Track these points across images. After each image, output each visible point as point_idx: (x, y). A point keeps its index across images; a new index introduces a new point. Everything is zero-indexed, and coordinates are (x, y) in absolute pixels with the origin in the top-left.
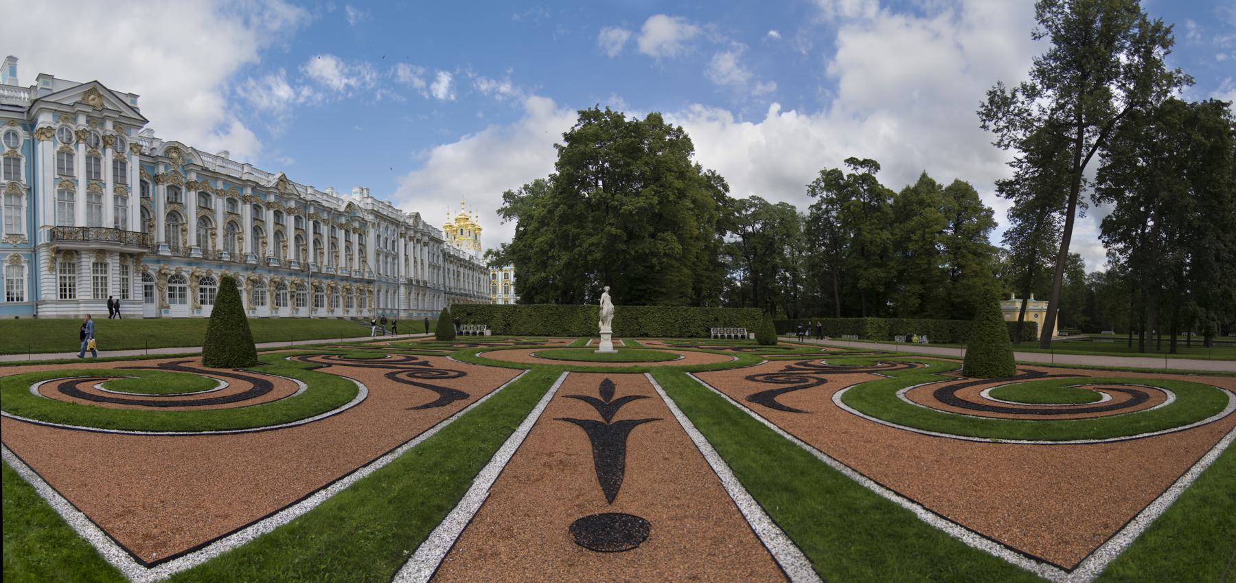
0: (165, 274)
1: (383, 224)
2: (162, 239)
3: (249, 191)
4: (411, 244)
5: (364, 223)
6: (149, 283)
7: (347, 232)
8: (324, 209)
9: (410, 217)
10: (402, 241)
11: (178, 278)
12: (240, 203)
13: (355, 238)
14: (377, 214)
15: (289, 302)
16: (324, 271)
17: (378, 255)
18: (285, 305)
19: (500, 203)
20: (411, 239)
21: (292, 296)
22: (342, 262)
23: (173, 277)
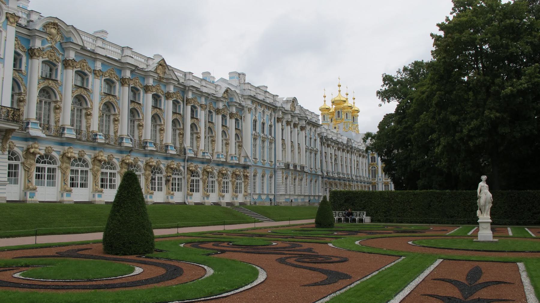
0: (34, 154)
1: (260, 109)
2: (33, 115)
3: (128, 74)
4: (288, 129)
5: (241, 108)
6: (14, 162)
7: (224, 117)
8: (202, 94)
9: (287, 101)
10: (279, 126)
11: (47, 158)
12: (118, 85)
13: (231, 123)
14: (253, 99)
15: (164, 187)
16: (200, 155)
17: (255, 139)
18: (160, 189)
20: (288, 123)
21: (167, 181)
22: (219, 146)
23: (41, 157)
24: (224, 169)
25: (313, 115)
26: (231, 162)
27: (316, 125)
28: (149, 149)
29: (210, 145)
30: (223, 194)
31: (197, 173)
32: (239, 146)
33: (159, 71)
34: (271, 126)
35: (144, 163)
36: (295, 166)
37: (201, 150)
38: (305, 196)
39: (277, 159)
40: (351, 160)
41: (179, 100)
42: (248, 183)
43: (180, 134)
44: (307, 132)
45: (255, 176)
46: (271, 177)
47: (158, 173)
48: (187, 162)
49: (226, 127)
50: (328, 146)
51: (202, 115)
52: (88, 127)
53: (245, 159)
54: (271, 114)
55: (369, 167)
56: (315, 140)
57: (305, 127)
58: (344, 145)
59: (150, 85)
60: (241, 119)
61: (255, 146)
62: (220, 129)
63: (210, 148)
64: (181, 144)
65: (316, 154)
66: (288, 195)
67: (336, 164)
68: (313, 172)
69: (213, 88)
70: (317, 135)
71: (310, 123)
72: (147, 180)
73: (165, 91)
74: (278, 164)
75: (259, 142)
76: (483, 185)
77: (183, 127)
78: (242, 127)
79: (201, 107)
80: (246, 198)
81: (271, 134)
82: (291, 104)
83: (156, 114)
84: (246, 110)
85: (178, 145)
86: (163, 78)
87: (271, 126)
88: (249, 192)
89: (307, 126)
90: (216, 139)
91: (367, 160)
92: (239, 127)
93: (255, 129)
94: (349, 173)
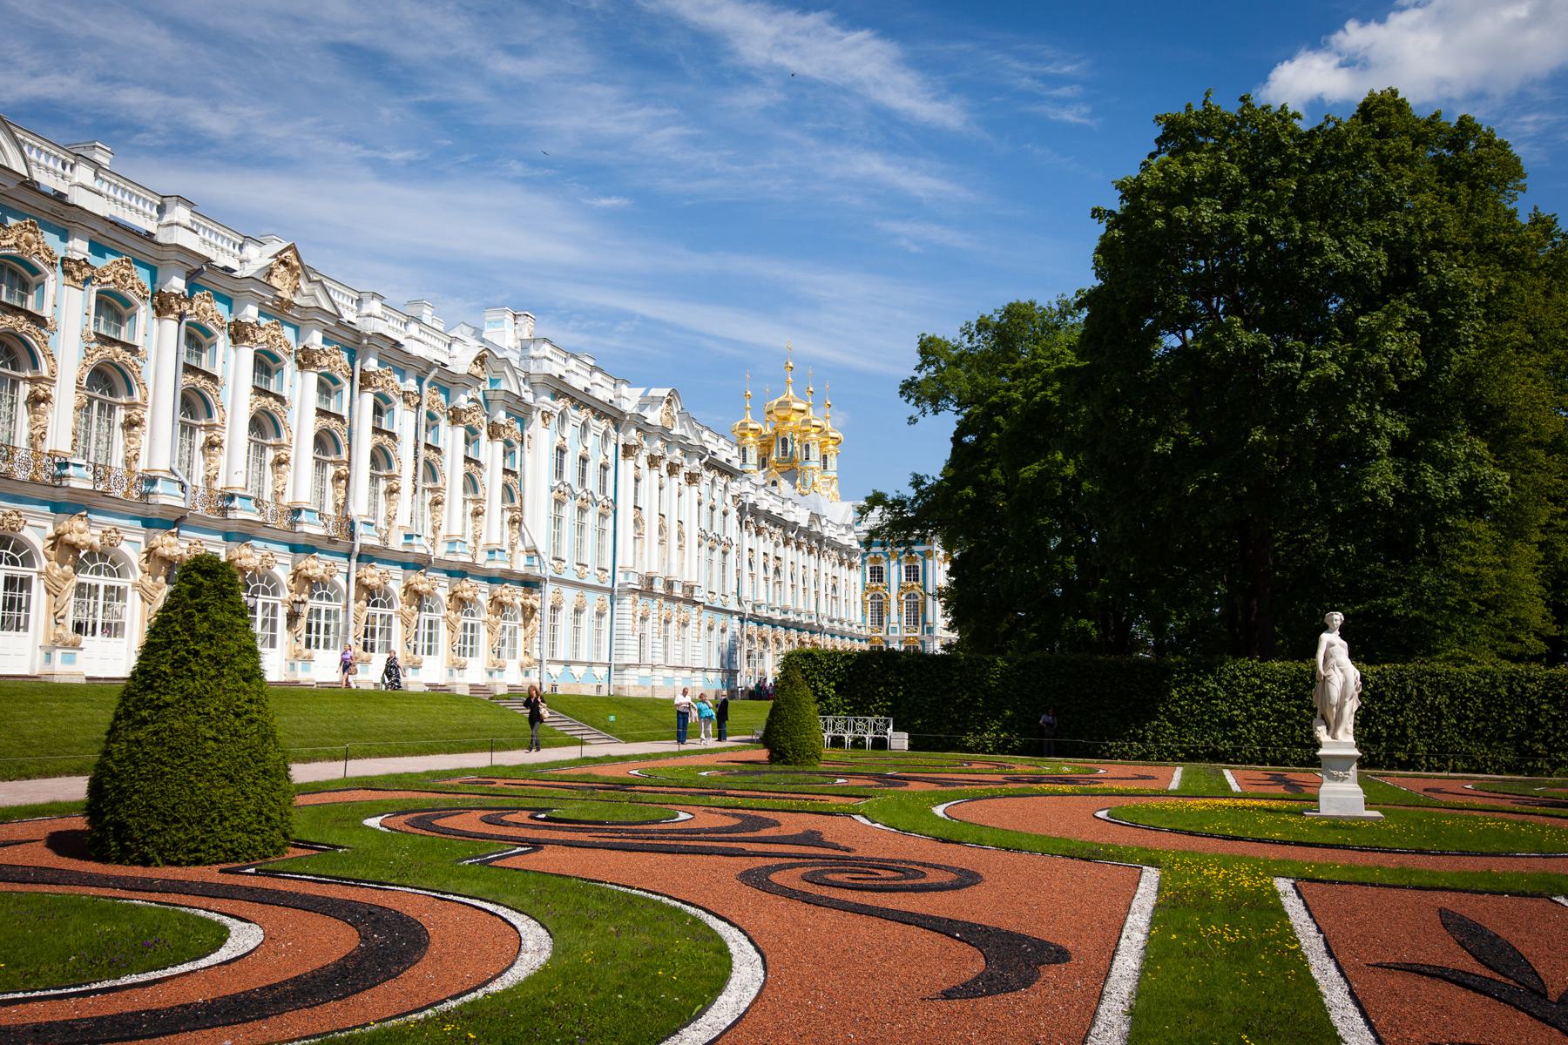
1: (577, 416)
4: (651, 478)
7: (471, 436)
10: (627, 468)
20: (653, 461)
21: (293, 617)
24: (467, 587)
26: (488, 566)
29: (428, 515)
31: (387, 595)
32: (513, 522)
36: (669, 585)
38: (694, 670)
39: (619, 563)
41: (338, 375)
43: (338, 478)
46: (600, 615)
47: (265, 592)
52: (35, 440)
61: (558, 521)
62: (460, 468)
69: (441, 345)
70: (729, 500)
74: (620, 578)
75: (570, 510)
76: (1332, 644)
79: (406, 401)
80: (527, 674)
81: (603, 490)
83: (264, 411)
84: (537, 417)
86: (290, 304)
87: (604, 467)
89: (705, 473)
90: (446, 497)
93: (559, 472)
94: (813, 609)
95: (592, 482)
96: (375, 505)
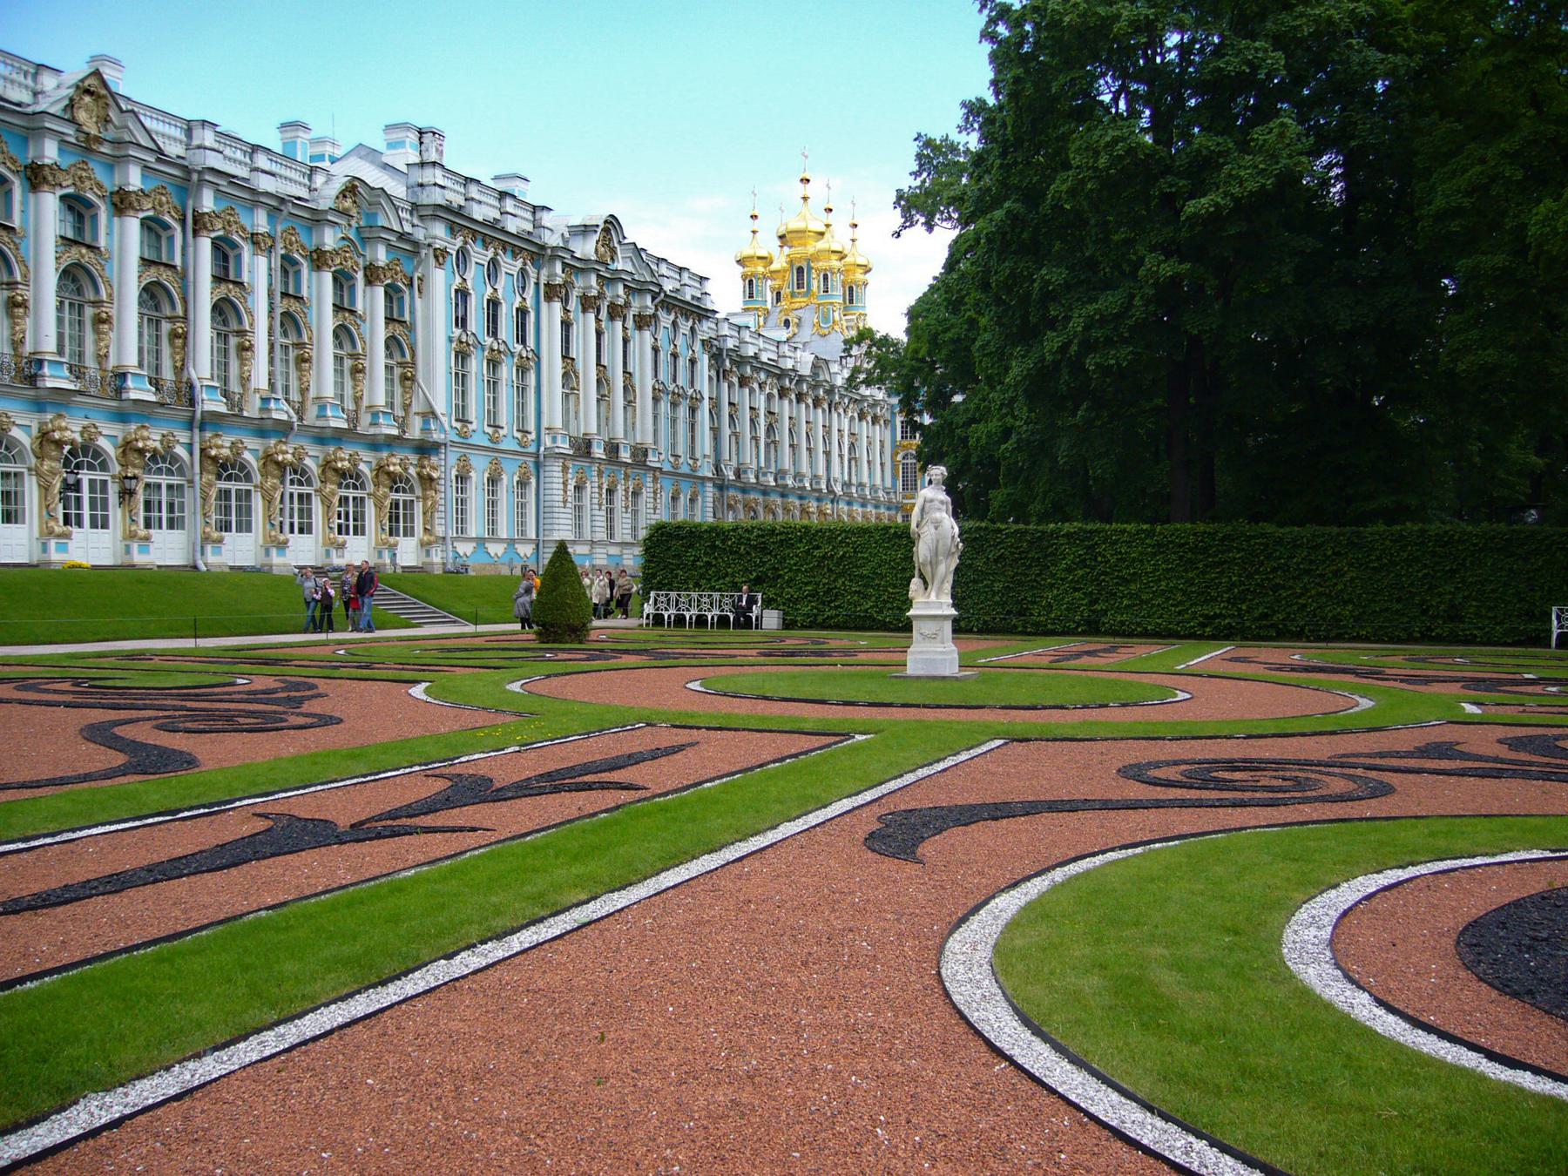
1: (480, 255)
5: (411, 247)
7: (342, 281)
8: (255, 198)
9: (585, 230)
14: (455, 217)
15: (116, 514)
16: (252, 410)
17: (462, 356)
18: (100, 523)
19: (903, 174)
20: (587, 303)
21: (126, 494)
22: (326, 378)
25: (685, 275)
26: (372, 431)
27: (697, 312)
28: (49, 385)
30: (341, 538)
33: (82, 116)
34: (522, 312)
35: (35, 432)
36: (613, 449)
37: (257, 390)
39: (545, 424)
40: (827, 429)
41: (167, 218)
42: (434, 503)
43: (174, 335)
44: (661, 335)
45: (462, 478)
46: (523, 484)
47: (91, 467)
48: (202, 429)
49: (352, 312)
50: (743, 381)
51: (257, 270)
53: (426, 422)
54: (523, 272)
55: (894, 454)
56: (693, 362)
57: (655, 316)
58: (801, 379)
59: (47, 161)
60: (411, 285)
61: (461, 378)
62: (329, 322)
63: (294, 385)
64: (180, 370)
65: (693, 410)
66: (585, 542)
67: (772, 444)
68: (685, 469)
70: (698, 347)
71: (670, 303)
72: (45, 489)
73: (110, 185)
75: (476, 366)
77: (186, 311)
78: (412, 312)
79: (255, 243)
81: (522, 339)
82: (596, 237)
85: (168, 374)
88: (439, 531)
89: (662, 314)
91: (888, 434)
92: (401, 313)
93: (462, 322)
94: (821, 471)
95: (507, 329)
96: (226, 365)
